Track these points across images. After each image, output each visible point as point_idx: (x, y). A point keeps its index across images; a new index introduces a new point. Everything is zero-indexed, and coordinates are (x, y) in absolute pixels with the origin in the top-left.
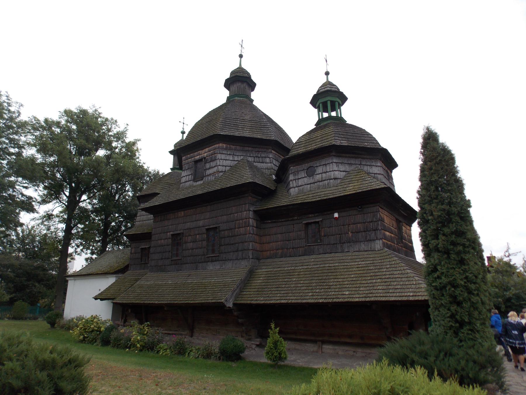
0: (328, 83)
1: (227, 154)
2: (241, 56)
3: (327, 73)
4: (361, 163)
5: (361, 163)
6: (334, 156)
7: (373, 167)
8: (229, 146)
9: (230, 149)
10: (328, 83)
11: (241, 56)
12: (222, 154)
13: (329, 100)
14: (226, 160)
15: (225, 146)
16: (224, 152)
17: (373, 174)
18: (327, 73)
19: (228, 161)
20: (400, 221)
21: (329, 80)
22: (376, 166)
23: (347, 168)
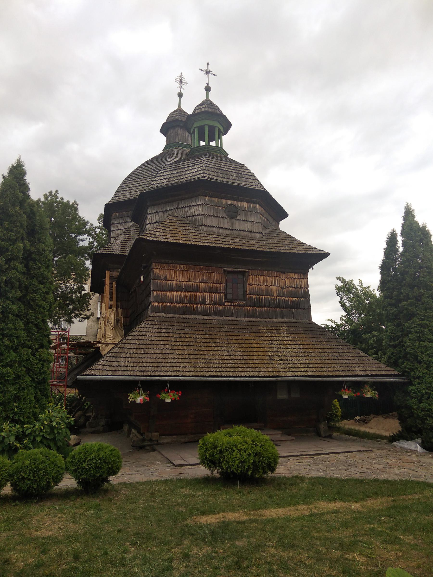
0: (207, 103)
1: (119, 223)
2: (180, 95)
3: (208, 89)
4: (178, 206)
5: (178, 206)
6: (149, 206)
7: (192, 207)
8: (121, 213)
9: (123, 217)
10: (207, 103)
11: (180, 95)
12: (115, 224)
13: (206, 125)
14: (118, 230)
15: (117, 214)
16: (116, 222)
17: (191, 217)
18: (208, 89)
19: (120, 231)
20: (243, 273)
21: (210, 98)
22: (196, 205)
23: (162, 216)
